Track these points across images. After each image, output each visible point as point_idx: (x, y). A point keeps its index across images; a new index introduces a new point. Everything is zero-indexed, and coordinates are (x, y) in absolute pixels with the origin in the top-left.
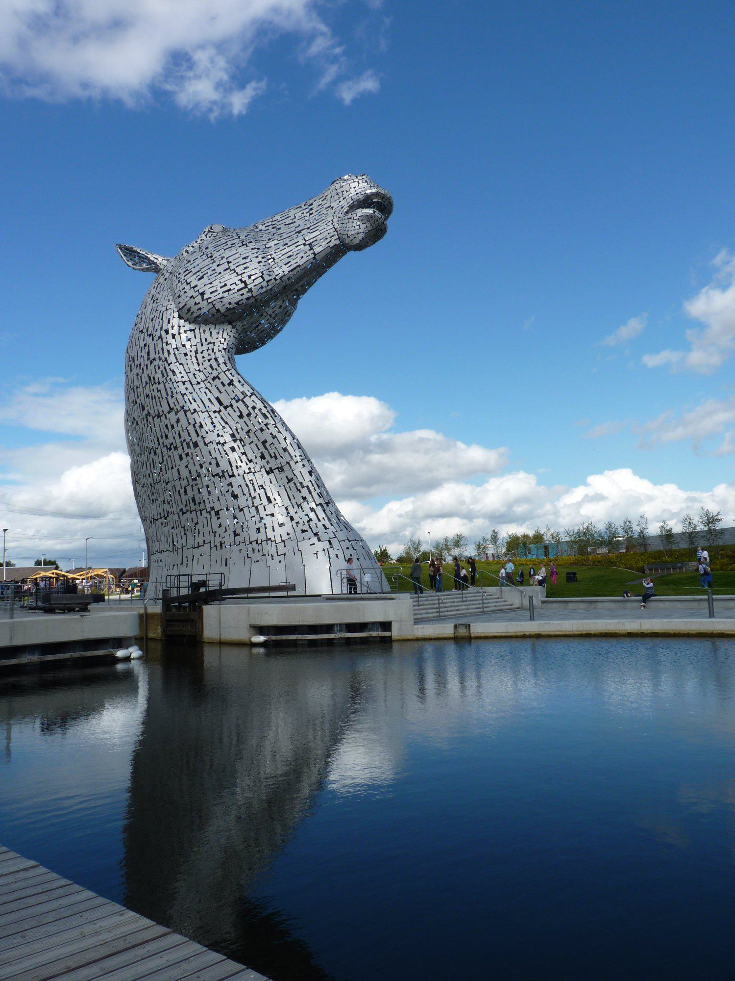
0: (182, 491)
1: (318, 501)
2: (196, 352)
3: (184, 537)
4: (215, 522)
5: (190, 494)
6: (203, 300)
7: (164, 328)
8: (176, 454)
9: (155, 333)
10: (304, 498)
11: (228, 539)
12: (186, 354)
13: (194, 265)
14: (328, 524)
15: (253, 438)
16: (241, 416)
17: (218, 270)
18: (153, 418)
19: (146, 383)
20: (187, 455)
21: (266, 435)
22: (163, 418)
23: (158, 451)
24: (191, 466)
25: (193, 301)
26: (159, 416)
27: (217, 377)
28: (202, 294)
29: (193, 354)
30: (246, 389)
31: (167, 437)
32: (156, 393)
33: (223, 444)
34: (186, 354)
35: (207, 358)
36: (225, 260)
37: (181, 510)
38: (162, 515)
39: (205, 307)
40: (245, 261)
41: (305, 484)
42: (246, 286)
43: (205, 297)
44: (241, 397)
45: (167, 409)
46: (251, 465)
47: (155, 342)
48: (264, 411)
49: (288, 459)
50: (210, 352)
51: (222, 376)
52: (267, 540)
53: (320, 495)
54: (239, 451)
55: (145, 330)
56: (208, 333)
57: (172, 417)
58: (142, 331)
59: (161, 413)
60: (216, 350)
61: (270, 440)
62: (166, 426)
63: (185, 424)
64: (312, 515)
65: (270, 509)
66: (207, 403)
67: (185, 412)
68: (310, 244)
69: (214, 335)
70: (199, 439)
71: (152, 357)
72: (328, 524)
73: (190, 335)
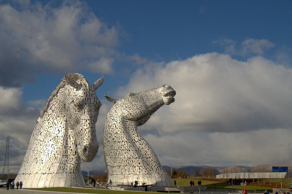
0: (125, 161)
1: (159, 165)
2: (128, 127)
3: (125, 172)
4: (134, 169)
5: (128, 162)
6: (131, 115)
7: (121, 120)
8: (124, 152)
9: (117, 122)
10: (156, 165)
11: (138, 173)
12: (126, 128)
13: (128, 105)
14: (161, 171)
15: (143, 150)
16: (140, 144)
17: (135, 108)
18: (117, 142)
19: (115, 133)
20: (127, 153)
21: (146, 149)
22: (120, 143)
23: (118, 150)
24: (128, 155)
25: (128, 115)
26: (119, 142)
27: (134, 134)
28: (131, 114)
29: (128, 128)
30: (141, 138)
31: (121, 148)
32: (118, 137)
33: (137, 151)
34: (126, 128)
35: (131, 129)
36: (136, 105)
37: (125, 165)
38: (118, 166)
39: (131, 117)
40: (141, 106)
41: (156, 161)
42: (142, 113)
43: (132, 115)
44: (140, 140)
45: (121, 141)
46: (143, 156)
47: (117, 124)
48: (146, 144)
49: (152, 155)
50: (132, 127)
51: (135, 134)
52: (148, 174)
53: (159, 164)
54: (140, 153)
55: (114, 120)
56: (131, 122)
57: (123, 143)
58: (113, 120)
59: (120, 142)
60: (133, 127)
61: (147, 151)
62: (121, 145)
63: (127, 145)
64: (157, 168)
65: (148, 167)
66: (132, 141)
67: (127, 142)
68: (156, 103)
69: (133, 123)
70: (130, 149)
71: (117, 127)
72: (161, 171)
73: (127, 123)
